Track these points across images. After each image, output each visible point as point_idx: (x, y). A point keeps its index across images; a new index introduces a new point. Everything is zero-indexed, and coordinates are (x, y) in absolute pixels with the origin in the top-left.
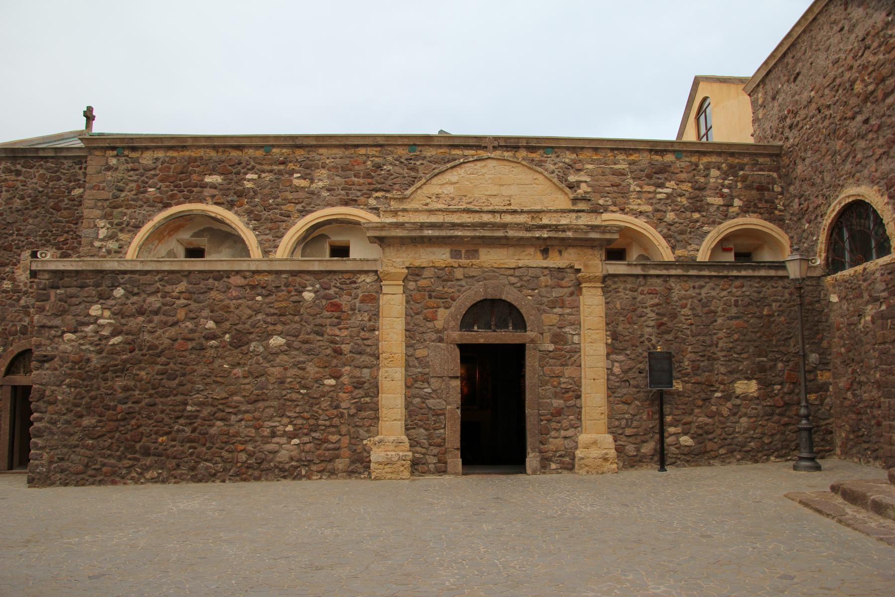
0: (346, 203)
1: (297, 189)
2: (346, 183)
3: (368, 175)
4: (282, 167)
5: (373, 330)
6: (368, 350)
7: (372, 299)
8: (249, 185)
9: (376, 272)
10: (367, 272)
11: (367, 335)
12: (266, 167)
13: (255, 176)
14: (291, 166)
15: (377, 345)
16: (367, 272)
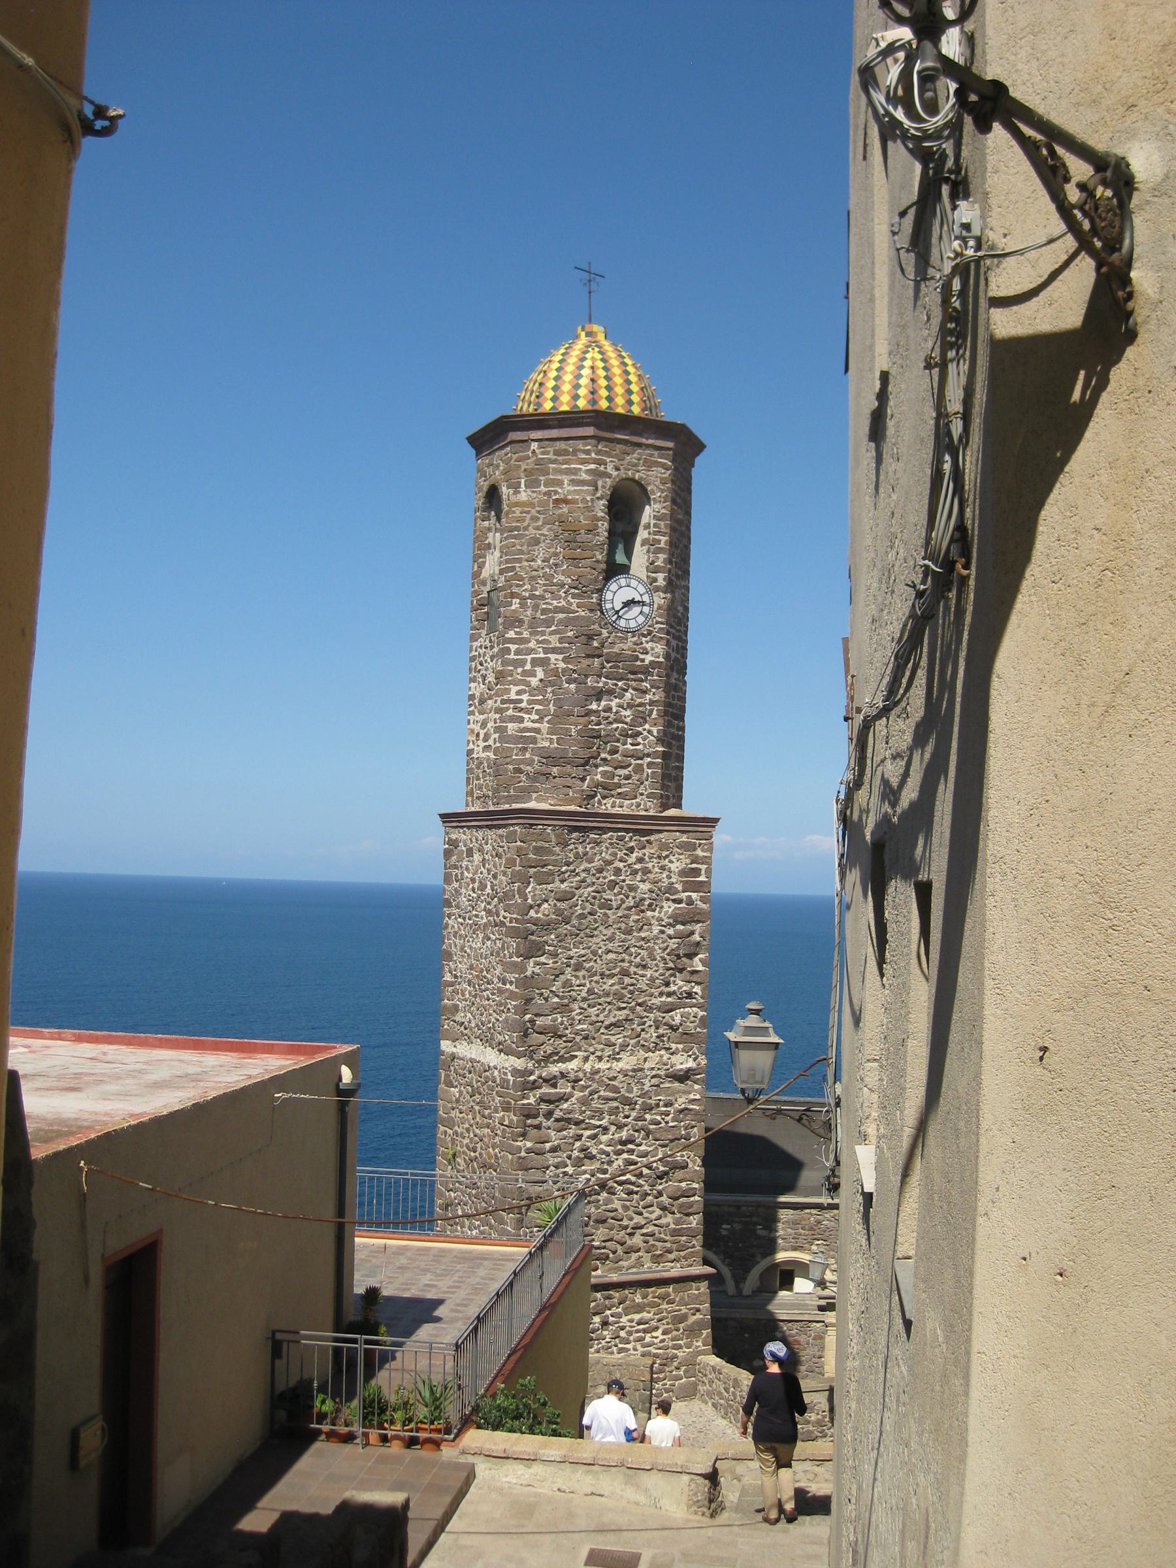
0: (795, 1249)
1: (759, 1237)
2: (796, 1233)
3: (811, 1229)
4: (748, 1219)
5: (820, 1357)
6: (817, 1370)
7: (820, 1337)
8: (724, 1233)
9: (823, 1322)
10: (818, 1322)
11: (817, 1360)
12: (736, 1219)
13: (729, 1227)
14: (755, 1219)
15: (823, 1367)
16: (818, 1322)
